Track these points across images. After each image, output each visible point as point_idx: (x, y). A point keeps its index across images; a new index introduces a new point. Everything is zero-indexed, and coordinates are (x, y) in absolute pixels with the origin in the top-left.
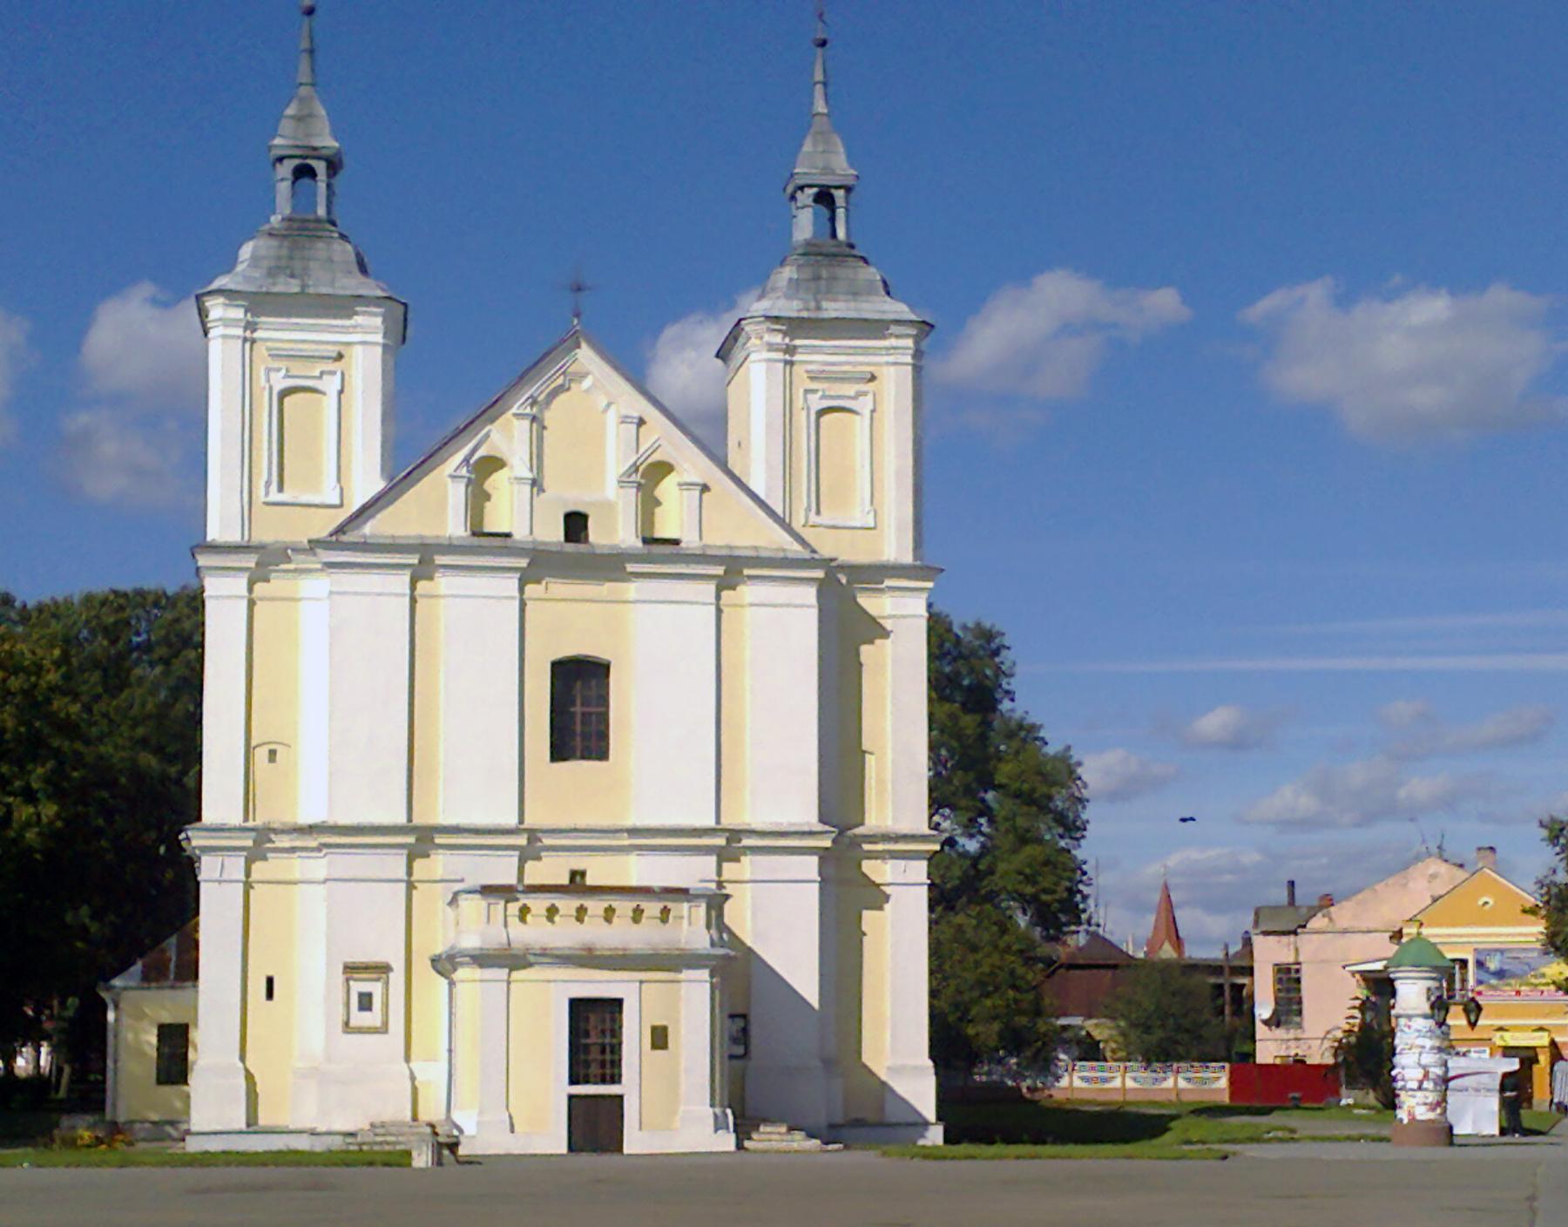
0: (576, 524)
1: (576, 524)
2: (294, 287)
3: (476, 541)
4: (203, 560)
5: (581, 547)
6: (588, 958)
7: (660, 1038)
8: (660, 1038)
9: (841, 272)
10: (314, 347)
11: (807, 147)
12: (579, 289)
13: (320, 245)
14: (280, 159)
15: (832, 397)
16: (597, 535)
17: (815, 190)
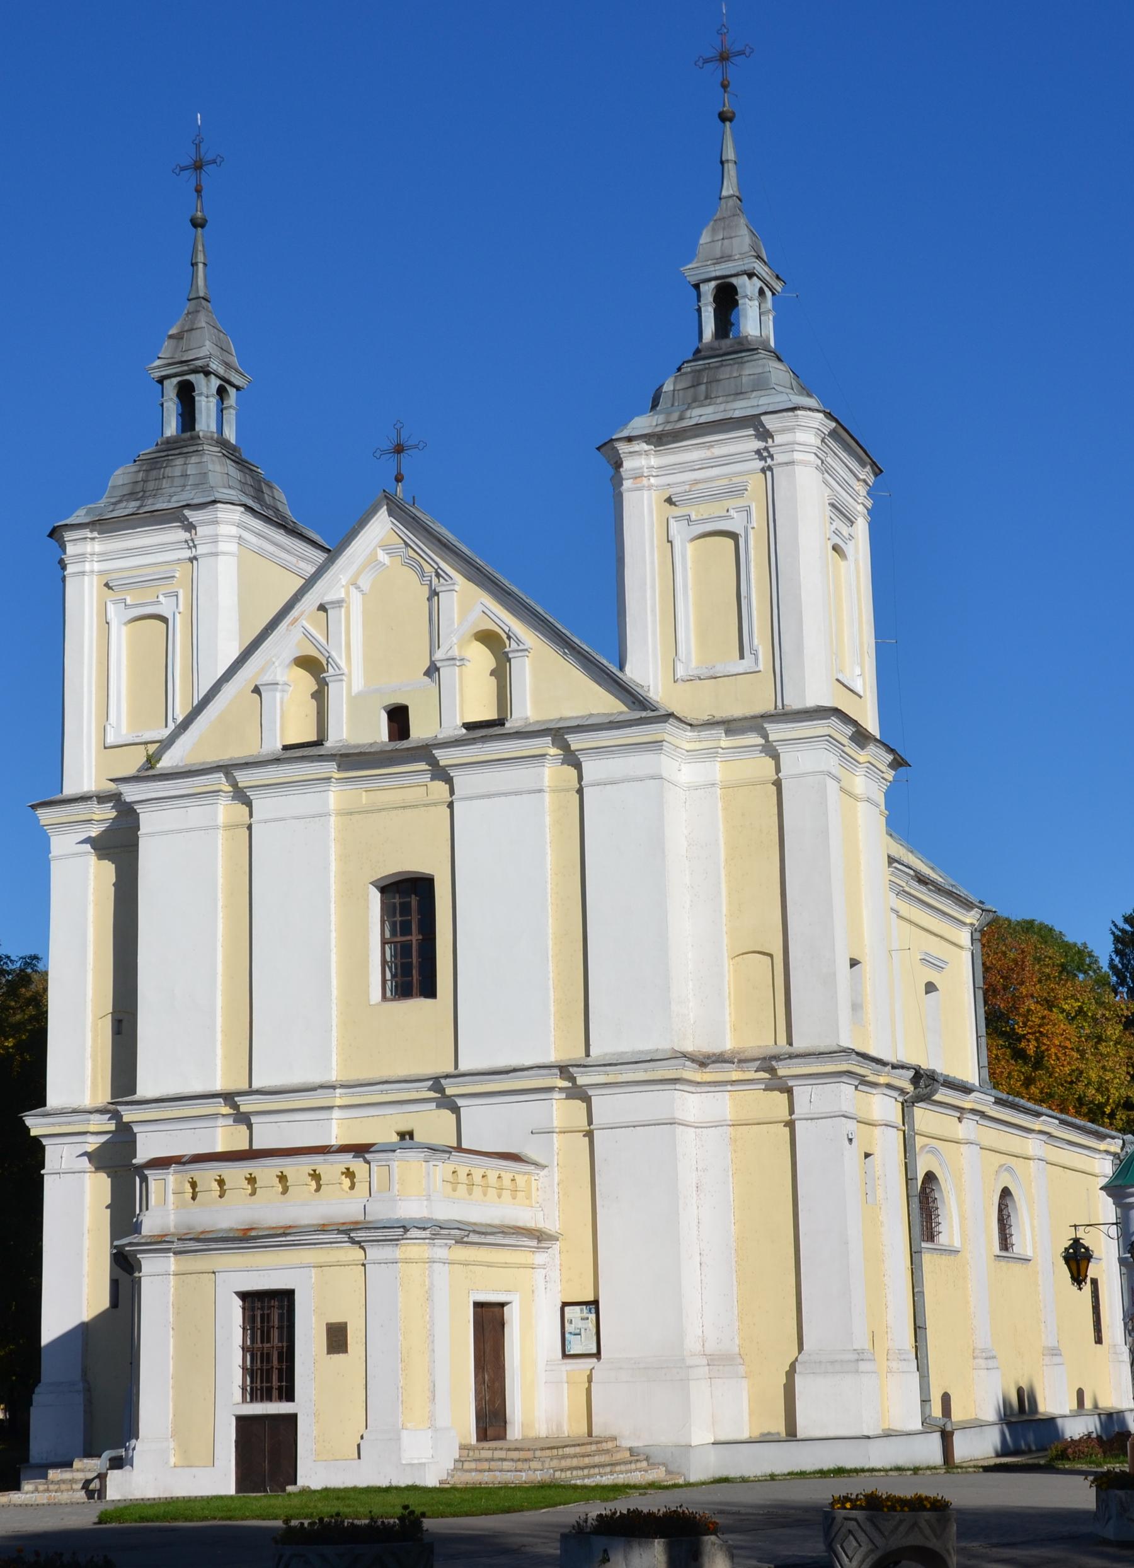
0: (398, 717)
1: (398, 717)
2: (132, 506)
3: (289, 754)
4: (46, 816)
5: (404, 744)
6: (245, 1238)
7: (337, 1338)
8: (337, 1338)
9: (725, 373)
10: (155, 569)
11: (705, 238)
12: (399, 449)
13: (179, 461)
14: (161, 381)
15: (704, 521)
16: (420, 730)
17: (713, 284)
